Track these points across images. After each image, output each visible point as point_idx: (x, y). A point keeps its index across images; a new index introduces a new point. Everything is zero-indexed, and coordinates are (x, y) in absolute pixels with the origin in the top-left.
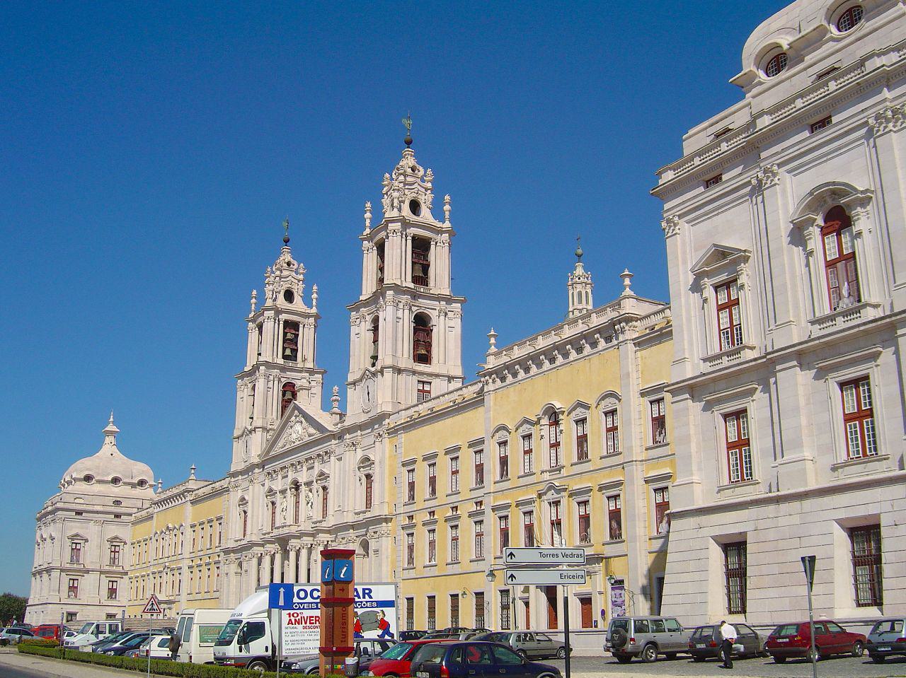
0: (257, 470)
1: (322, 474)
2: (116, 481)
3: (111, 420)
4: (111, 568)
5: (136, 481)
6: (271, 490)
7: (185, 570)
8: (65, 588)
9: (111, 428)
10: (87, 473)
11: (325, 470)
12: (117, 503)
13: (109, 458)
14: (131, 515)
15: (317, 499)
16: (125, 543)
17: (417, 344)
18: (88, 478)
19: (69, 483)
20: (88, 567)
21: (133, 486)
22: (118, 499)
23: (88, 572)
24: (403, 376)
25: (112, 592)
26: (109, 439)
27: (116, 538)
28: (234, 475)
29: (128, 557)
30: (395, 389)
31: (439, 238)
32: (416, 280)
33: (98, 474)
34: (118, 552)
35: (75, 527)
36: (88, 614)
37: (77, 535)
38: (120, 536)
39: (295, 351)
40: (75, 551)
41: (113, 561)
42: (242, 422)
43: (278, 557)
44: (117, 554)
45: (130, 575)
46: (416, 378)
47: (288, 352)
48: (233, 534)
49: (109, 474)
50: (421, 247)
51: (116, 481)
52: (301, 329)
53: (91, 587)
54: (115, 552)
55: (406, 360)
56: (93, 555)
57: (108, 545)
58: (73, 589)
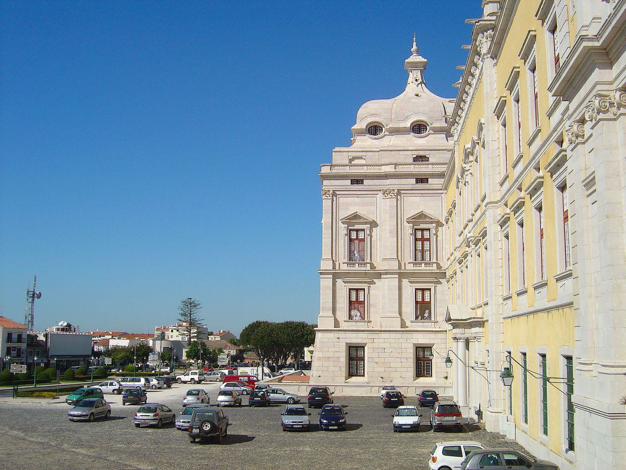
2: (419, 128)
3: (415, 47)
4: (417, 268)
9: (415, 58)
10: (370, 120)
12: (420, 159)
13: (416, 99)
18: (374, 129)
20: (380, 266)
22: (422, 153)
23: (379, 275)
34: (429, 240)
36: (384, 346)
41: (420, 255)
44: (426, 243)
51: (419, 128)
54: (423, 240)
56: (384, 247)
57: (408, 229)
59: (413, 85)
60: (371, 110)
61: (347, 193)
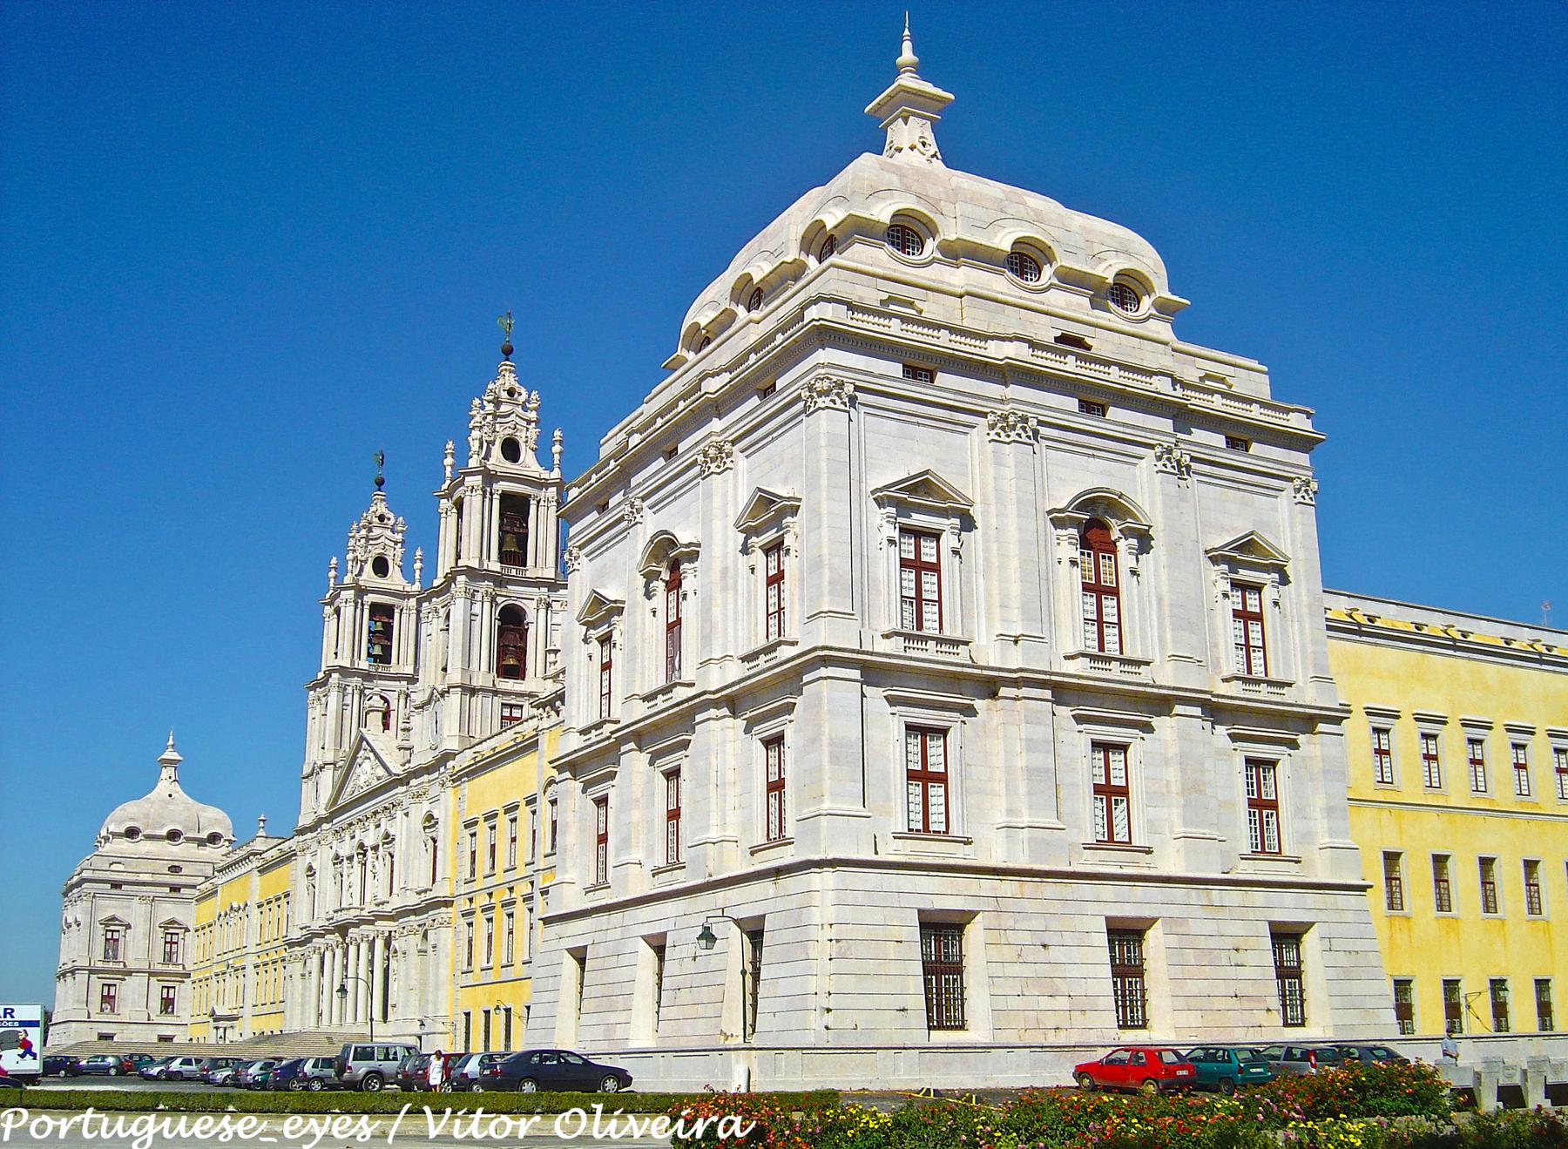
0: (325, 826)
1: (387, 835)
2: (173, 836)
4: (165, 968)
5: (204, 835)
6: (337, 857)
7: (250, 969)
8: (96, 998)
9: (170, 755)
10: (129, 824)
11: (392, 832)
12: (175, 869)
13: (167, 800)
14: (194, 887)
15: (382, 870)
16: (187, 930)
17: (502, 652)
18: (132, 833)
19: (107, 839)
20: (131, 965)
21: (201, 843)
23: (130, 973)
24: (477, 700)
25: (168, 1004)
26: (167, 772)
27: (173, 922)
28: (302, 832)
29: (191, 951)
30: (465, 719)
31: (542, 494)
32: (504, 557)
33: (148, 826)
35: (110, 907)
37: (113, 918)
38: (179, 918)
39: (387, 650)
40: (112, 944)
41: (169, 957)
42: (314, 755)
43: (339, 952)
45: (194, 977)
46: (498, 700)
47: (377, 650)
48: (301, 916)
49: (163, 826)
50: (515, 510)
51: (173, 836)
52: (397, 616)
53: (135, 995)
54: (171, 943)
55: (483, 676)
56: (137, 948)
57: (160, 933)
58: (108, 999)
59: (166, 783)
60: (126, 813)
61: (109, 896)
